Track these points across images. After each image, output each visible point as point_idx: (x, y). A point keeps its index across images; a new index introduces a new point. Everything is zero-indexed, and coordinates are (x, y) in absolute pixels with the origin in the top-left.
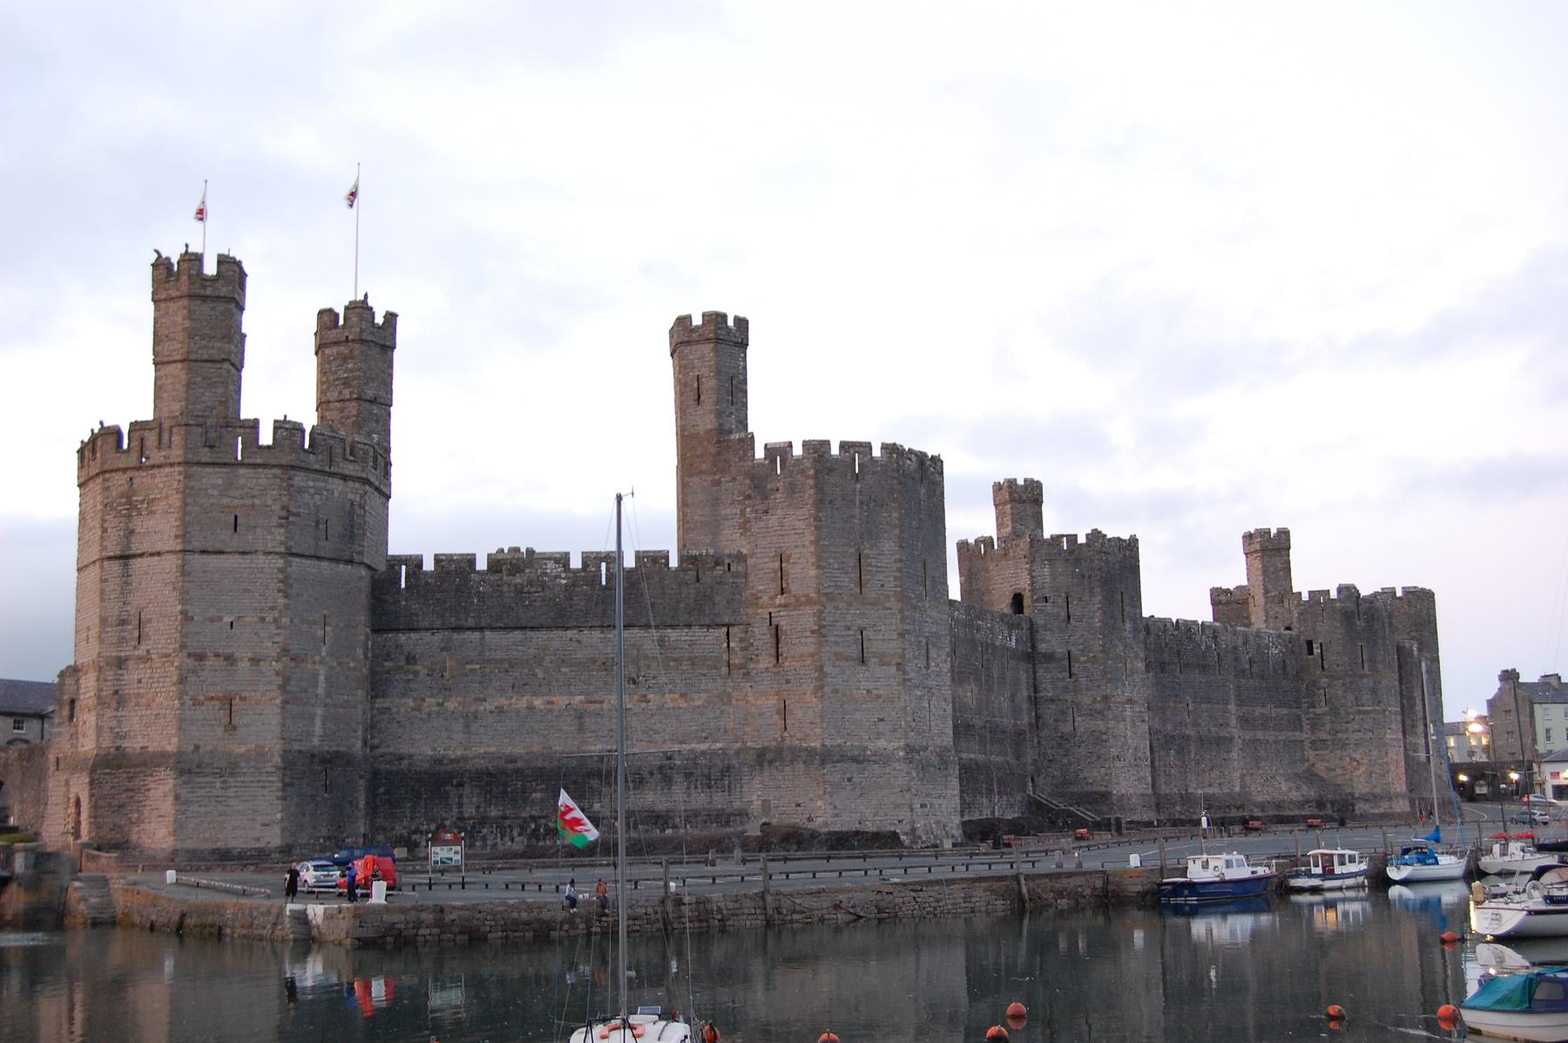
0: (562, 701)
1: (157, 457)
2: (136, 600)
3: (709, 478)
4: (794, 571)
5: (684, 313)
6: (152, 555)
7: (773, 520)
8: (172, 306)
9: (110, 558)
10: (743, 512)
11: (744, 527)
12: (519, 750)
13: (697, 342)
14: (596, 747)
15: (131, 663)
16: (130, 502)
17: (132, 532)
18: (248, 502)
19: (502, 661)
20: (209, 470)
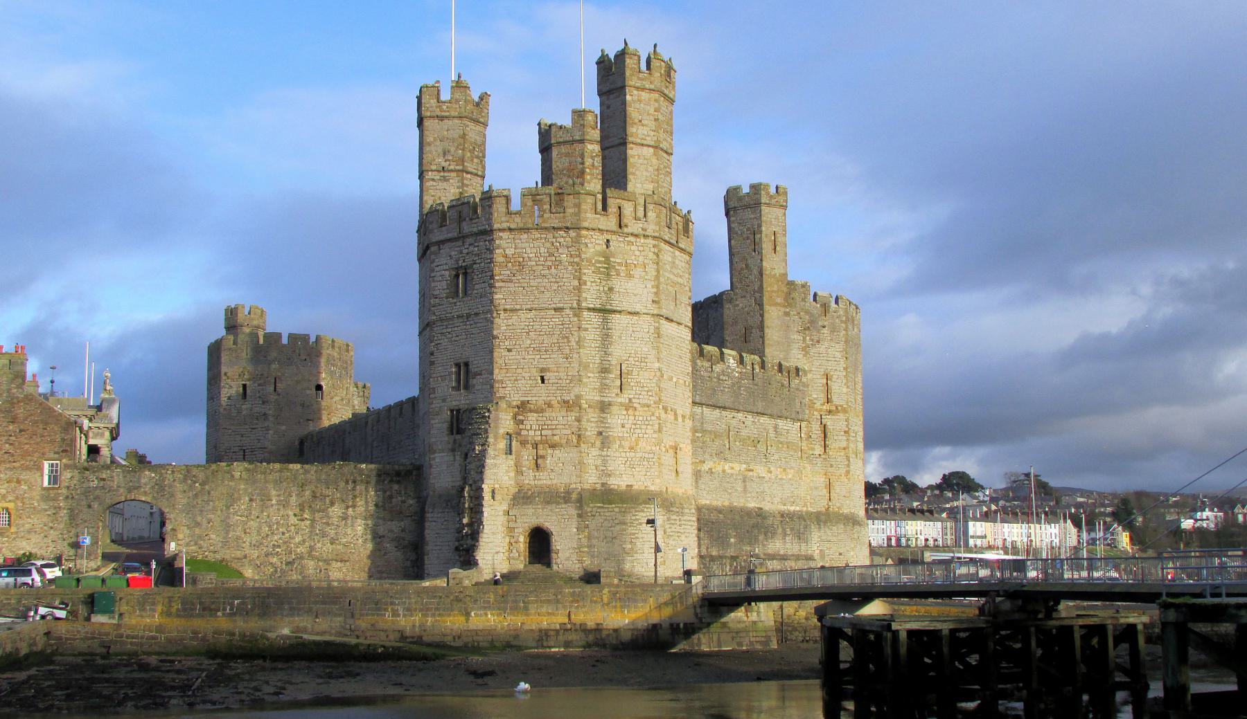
0: (737, 466)
1: (634, 227)
2: (618, 352)
3: (783, 309)
4: (835, 387)
5: (763, 181)
6: (630, 313)
7: (822, 348)
8: (644, 95)
9: (589, 309)
10: (804, 339)
11: (805, 350)
12: (719, 504)
13: (775, 206)
14: (752, 505)
15: (614, 409)
16: (607, 258)
17: (611, 289)
18: (680, 280)
19: (710, 432)
20: (667, 247)
